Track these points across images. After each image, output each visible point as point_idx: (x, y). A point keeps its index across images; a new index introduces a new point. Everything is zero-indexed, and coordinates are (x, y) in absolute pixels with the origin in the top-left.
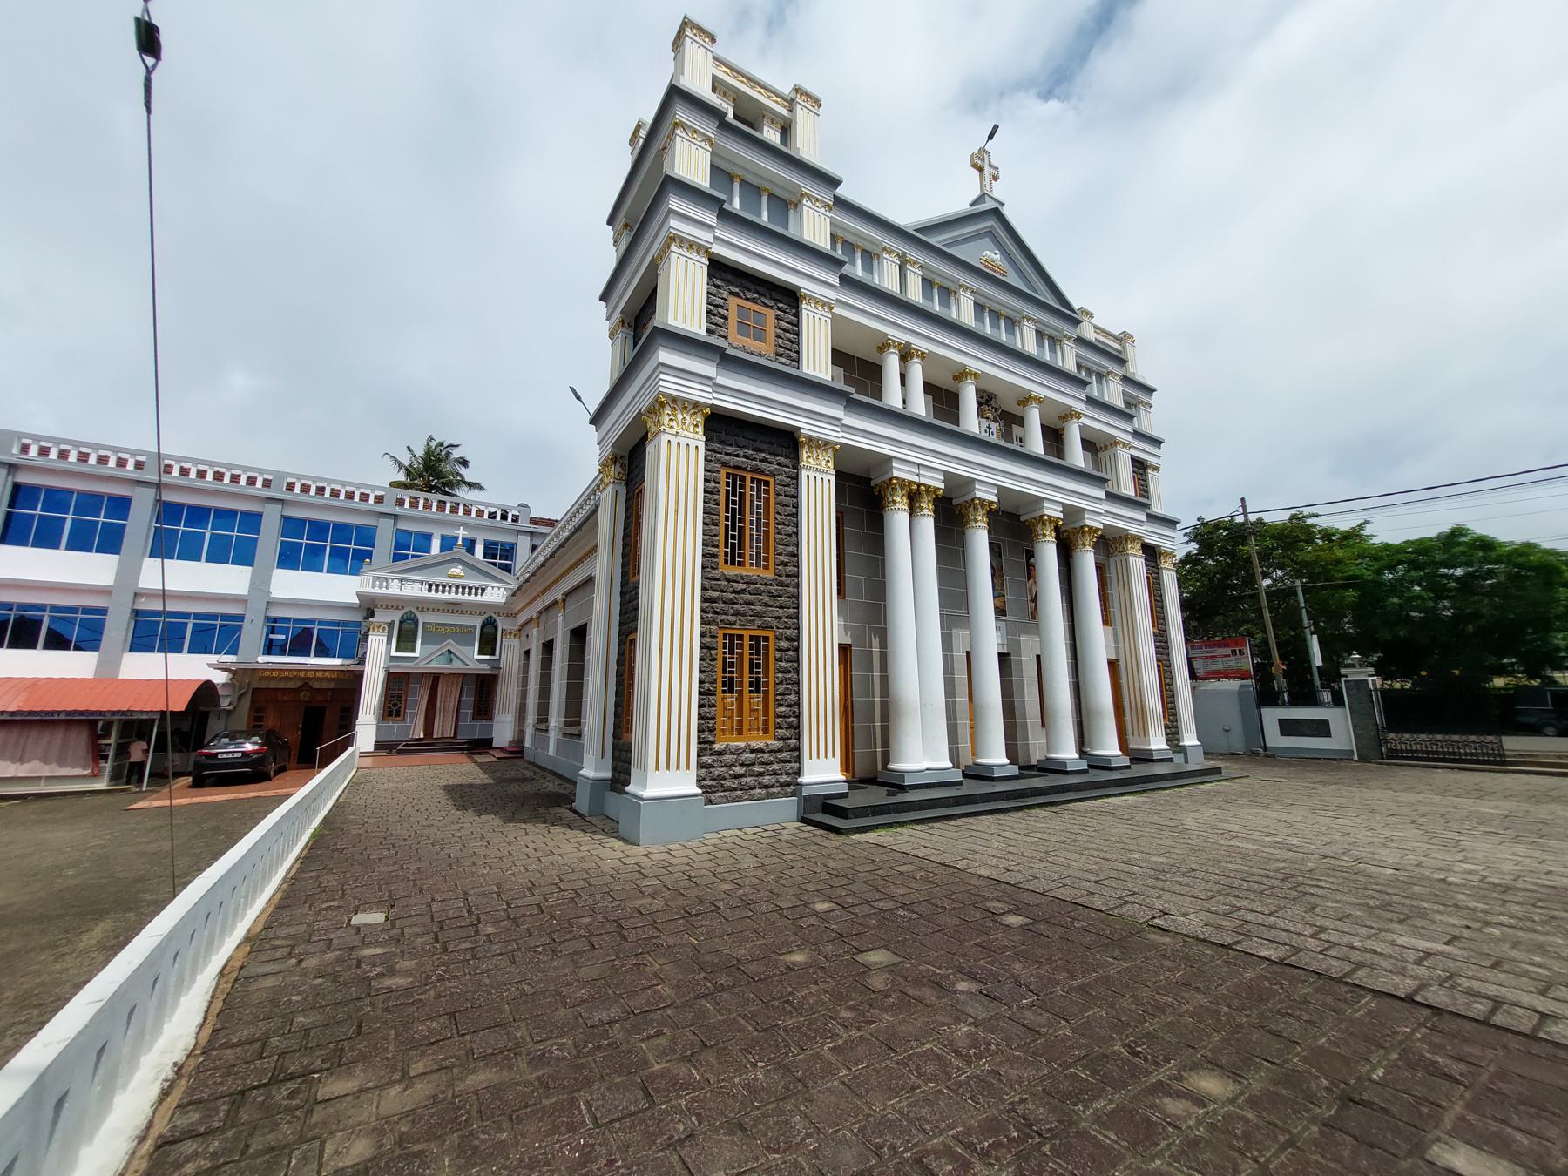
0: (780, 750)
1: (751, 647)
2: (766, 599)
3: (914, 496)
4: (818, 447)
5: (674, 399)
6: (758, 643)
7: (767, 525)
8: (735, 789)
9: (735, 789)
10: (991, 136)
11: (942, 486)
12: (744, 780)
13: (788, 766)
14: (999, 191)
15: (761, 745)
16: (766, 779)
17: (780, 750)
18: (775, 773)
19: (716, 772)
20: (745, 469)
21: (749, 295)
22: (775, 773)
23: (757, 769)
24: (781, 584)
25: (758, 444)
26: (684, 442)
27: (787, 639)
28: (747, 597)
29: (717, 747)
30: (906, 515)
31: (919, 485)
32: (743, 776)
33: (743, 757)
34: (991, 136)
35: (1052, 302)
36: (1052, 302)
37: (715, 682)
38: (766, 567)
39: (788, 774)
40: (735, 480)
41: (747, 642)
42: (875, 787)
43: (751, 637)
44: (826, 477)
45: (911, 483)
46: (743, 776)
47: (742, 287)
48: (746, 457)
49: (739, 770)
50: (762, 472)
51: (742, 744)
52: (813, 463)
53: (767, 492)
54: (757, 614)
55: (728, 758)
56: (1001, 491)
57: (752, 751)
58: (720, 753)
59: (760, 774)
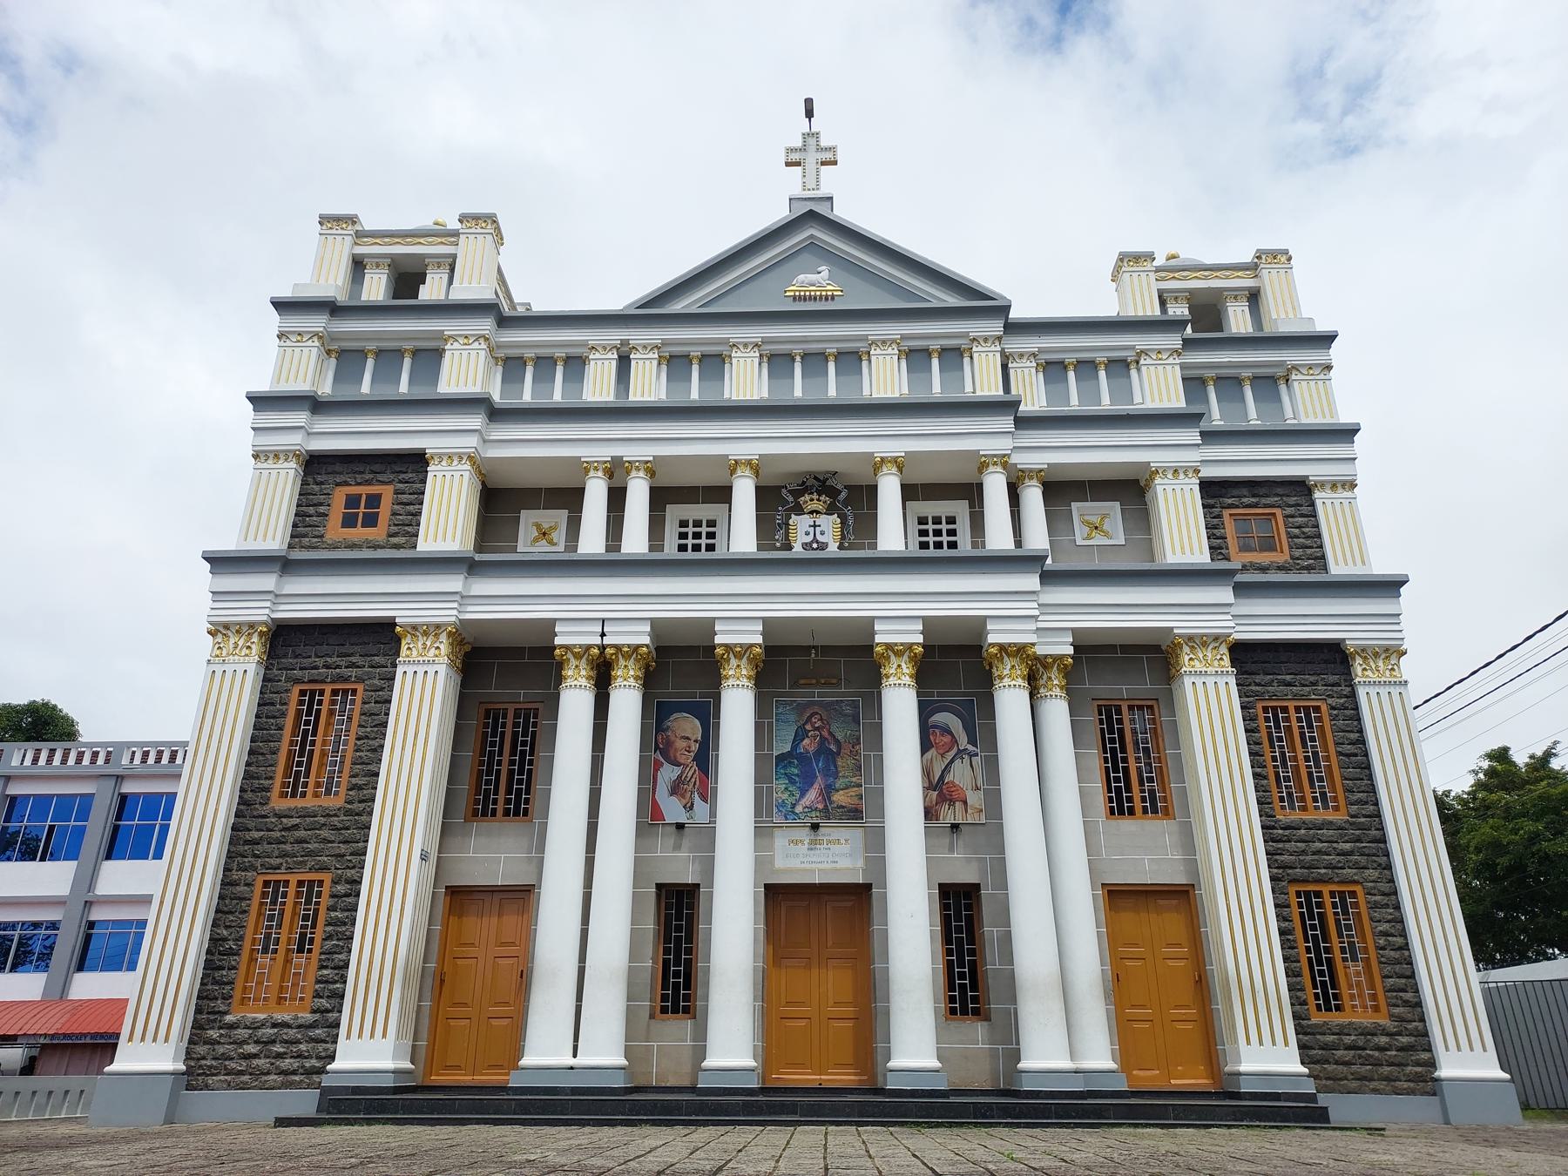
0: (313, 1026)
1: (1334, 905)
2: (324, 833)
3: (1035, 671)
4: (1205, 645)
5: (415, 627)
6: (309, 889)
7: (1327, 759)
8: (241, 1073)
9: (241, 1073)
10: (809, 114)
11: (646, 640)
12: (255, 1062)
13: (321, 1047)
14: (830, 181)
15: (287, 1017)
16: (286, 1063)
17: (313, 1026)
18: (300, 1056)
19: (221, 1050)
20: (323, 682)
21: (359, 478)
22: (300, 1056)
23: (278, 1048)
24: (348, 813)
25: (343, 650)
26: (229, 668)
27: (347, 882)
28: (302, 833)
29: (229, 1018)
30: (1024, 695)
31: (603, 648)
32: (255, 1056)
33: (260, 1033)
34: (809, 114)
35: (952, 300)
36: (952, 300)
37: (241, 938)
38: (1336, 809)
39: (319, 1058)
40: (1109, 716)
41: (1328, 900)
42: (464, 1084)
43: (1332, 894)
44: (1221, 681)
45: (589, 647)
46: (255, 1056)
47: (382, 468)
48: (327, 667)
49: (251, 1048)
50: (346, 680)
51: (262, 1016)
52: (1198, 666)
53: (1319, 719)
54: (311, 854)
55: (242, 1033)
56: (929, 624)
57: (274, 1025)
58: (232, 1026)
59: (280, 1056)
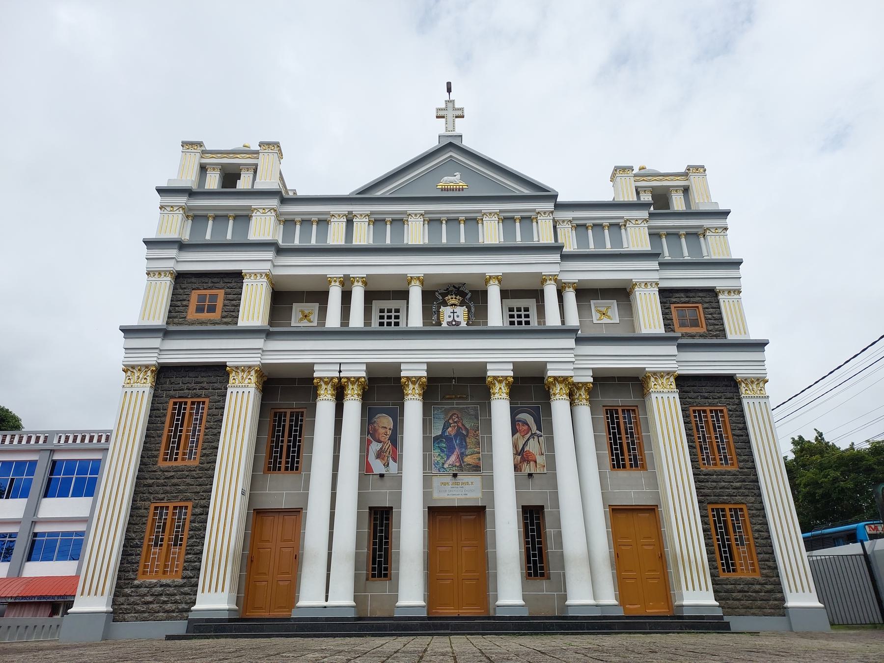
0: (182, 586)
1: (732, 516)
2: (188, 480)
3: (573, 390)
4: (662, 377)
5: (237, 367)
7: (727, 438)
8: (144, 612)
9: (144, 612)
10: (449, 90)
11: (364, 374)
12: (151, 606)
13: (187, 597)
14: (460, 127)
15: (168, 581)
16: (168, 606)
17: (182, 586)
18: (176, 602)
19: (132, 599)
22: (176, 602)
23: (164, 598)
24: (201, 469)
25: (197, 380)
26: (135, 390)
27: (201, 507)
28: (175, 481)
29: (136, 582)
30: (567, 404)
31: (340, 378)
32: (151, 603)
33: (154, 590)
34: (449, 90)
36: (526, 192)
37: (143, 538)
38: (732, 464)
39: (186, 603)
40: (611, 413)
41: (728, 513)
43: (730, 510)
44: (671, 396)
45: (332, 378)
46: (151, 603)
49: (149, 599)
50: (199, 396)
51: (155, 581)
52: (659, 388)
53: (723, 417)
54: (181, 492)
55: (144, 590)
57: (161, 586)
58: (138, 587)
59: (165, 602)
